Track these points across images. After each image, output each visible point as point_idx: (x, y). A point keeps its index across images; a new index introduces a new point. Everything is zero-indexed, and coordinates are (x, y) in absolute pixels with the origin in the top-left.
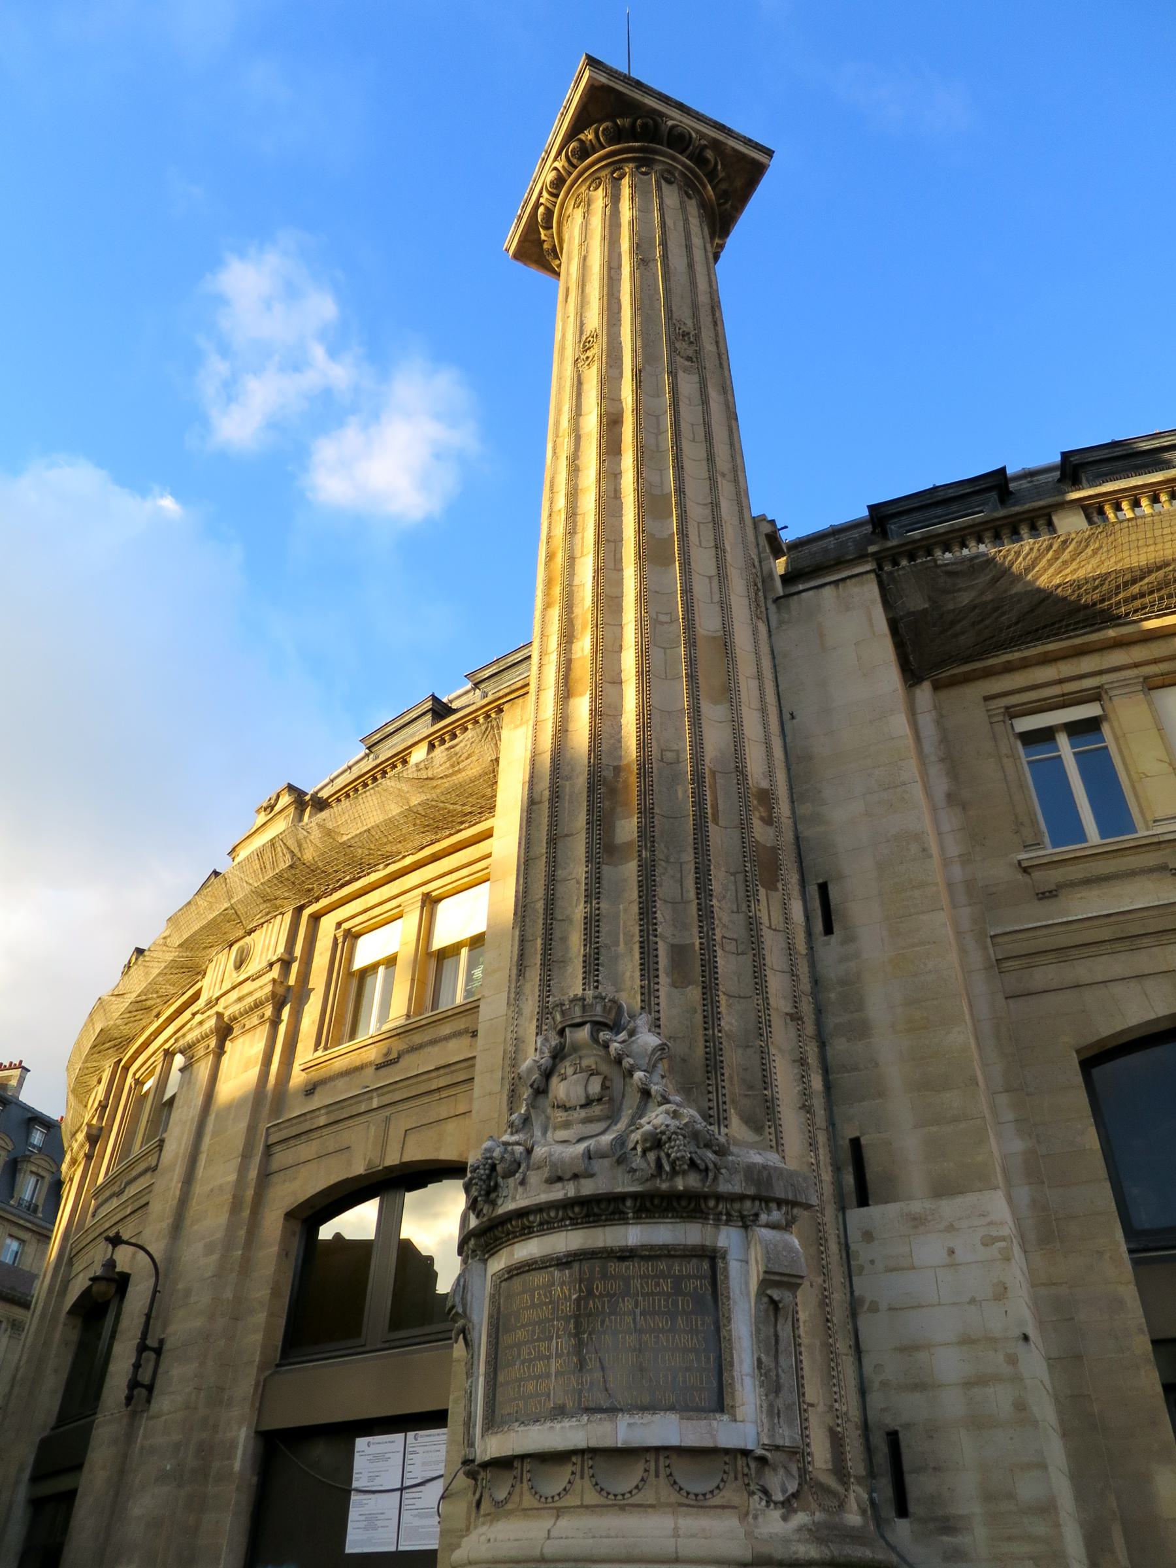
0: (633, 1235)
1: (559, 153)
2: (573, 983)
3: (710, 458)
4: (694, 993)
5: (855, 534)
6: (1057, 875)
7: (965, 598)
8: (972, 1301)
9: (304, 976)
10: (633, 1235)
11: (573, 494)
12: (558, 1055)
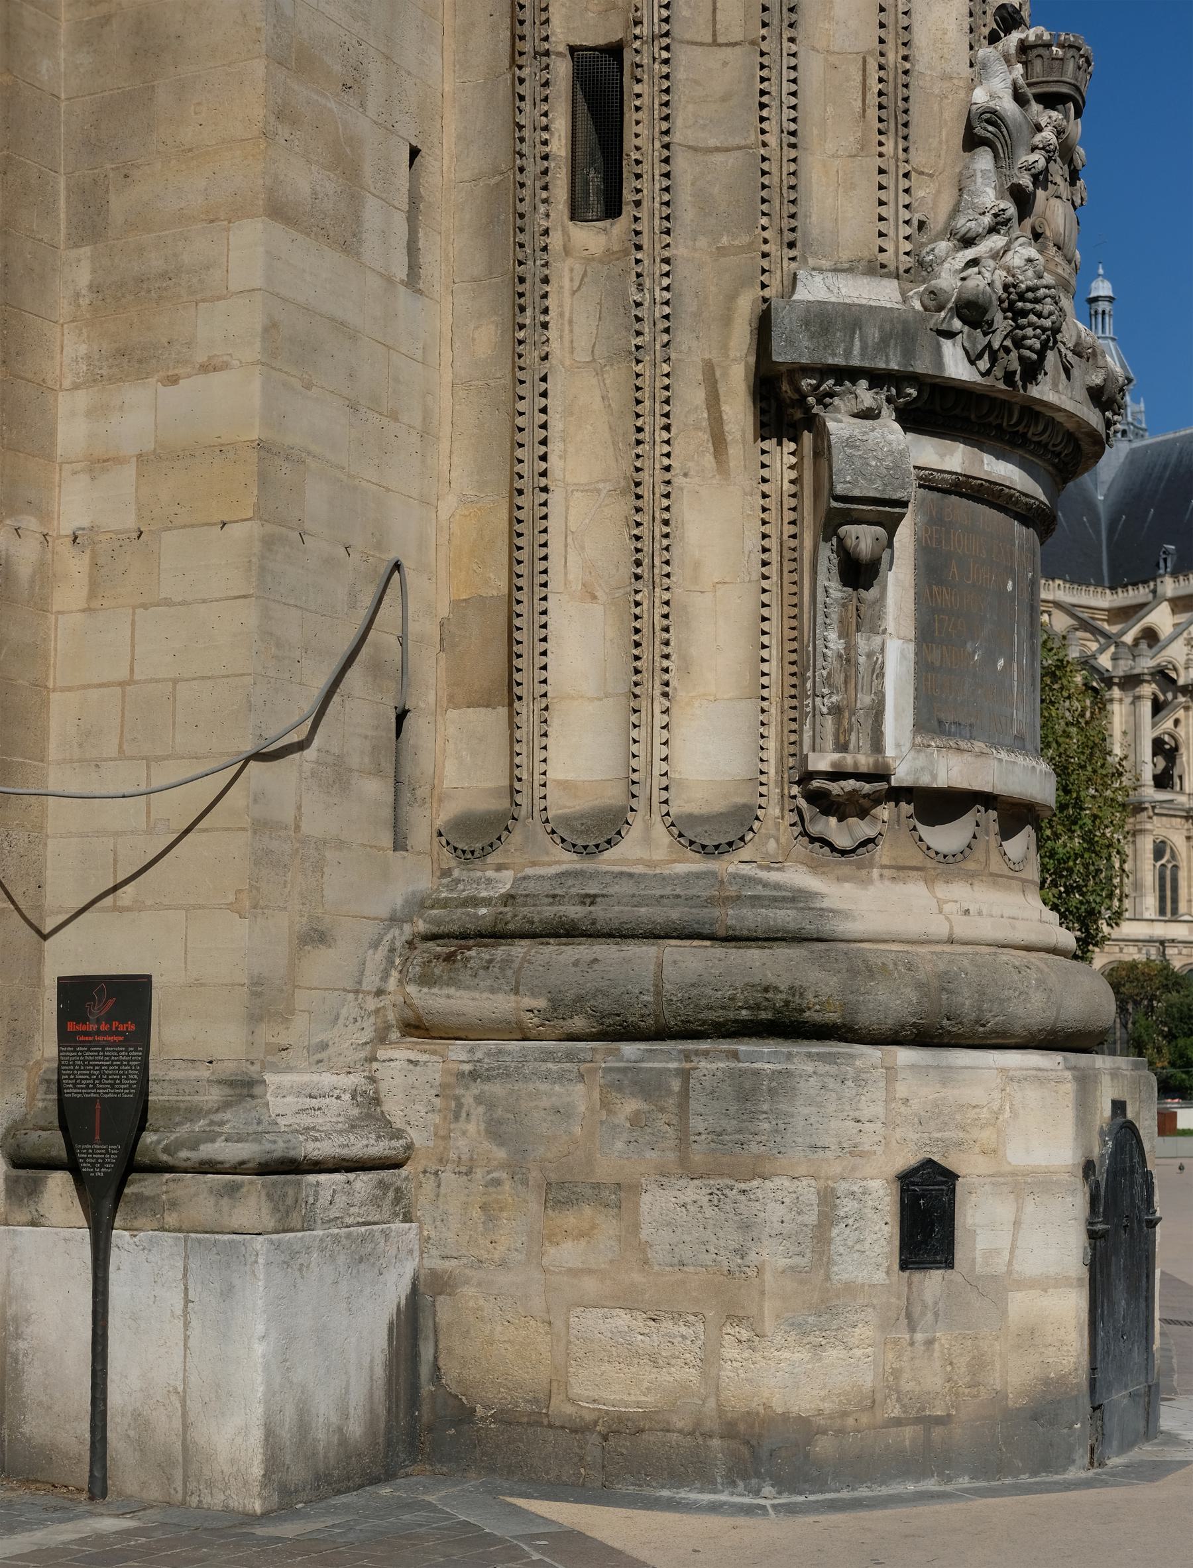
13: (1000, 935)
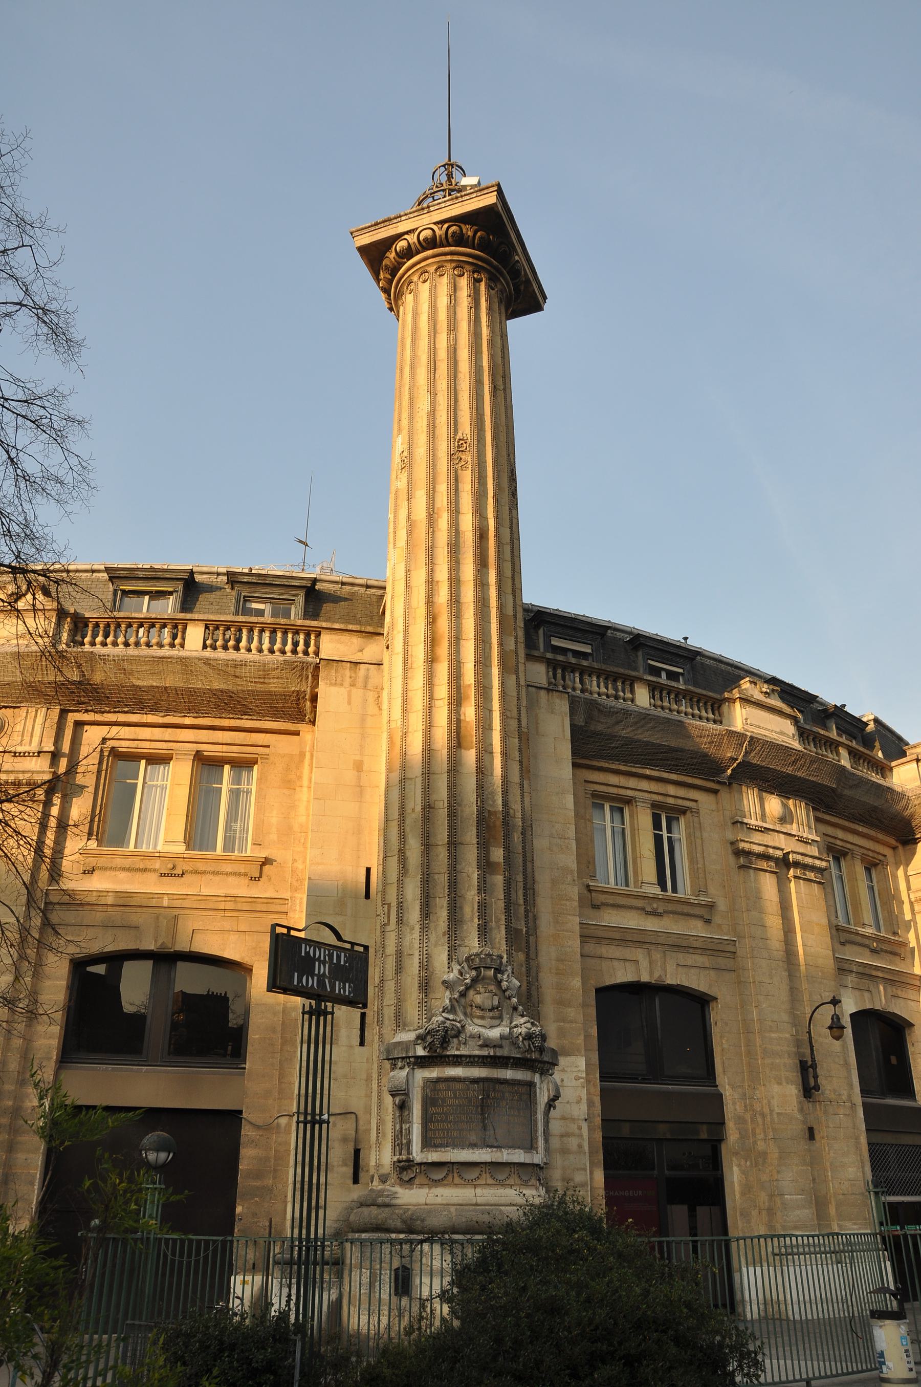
0: (509, 1074)
1: (442, 222)
6: (602, 898)
7: (600, 728)
8: (568, 1102)
10: (509, 1074)
11: (455, 582)
12: (475, 981)
13: (444, 1202)
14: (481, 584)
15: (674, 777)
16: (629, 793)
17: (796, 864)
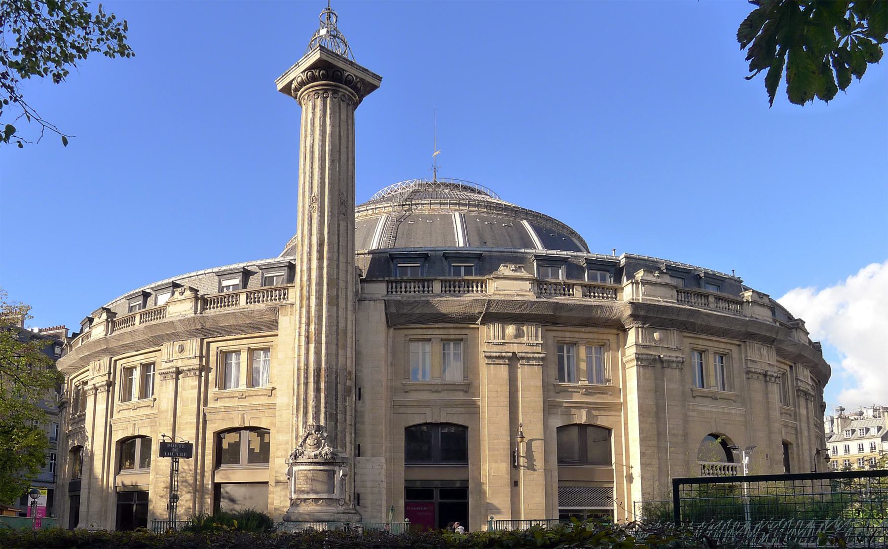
2: (311, 421)
3: (347, 262)
4: (333, 423)
5: (384, 255)
6: (409, 388)
7: (405, 311)
9: (208, 362)
11: (309, 270)
12: (309, 434)
14: (320, 268)
15: (452, 326)
16: (429, 337)
17: (522, 358)
